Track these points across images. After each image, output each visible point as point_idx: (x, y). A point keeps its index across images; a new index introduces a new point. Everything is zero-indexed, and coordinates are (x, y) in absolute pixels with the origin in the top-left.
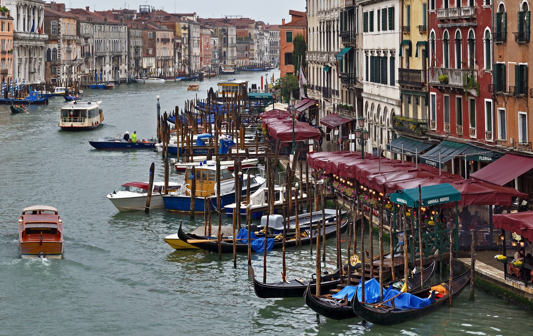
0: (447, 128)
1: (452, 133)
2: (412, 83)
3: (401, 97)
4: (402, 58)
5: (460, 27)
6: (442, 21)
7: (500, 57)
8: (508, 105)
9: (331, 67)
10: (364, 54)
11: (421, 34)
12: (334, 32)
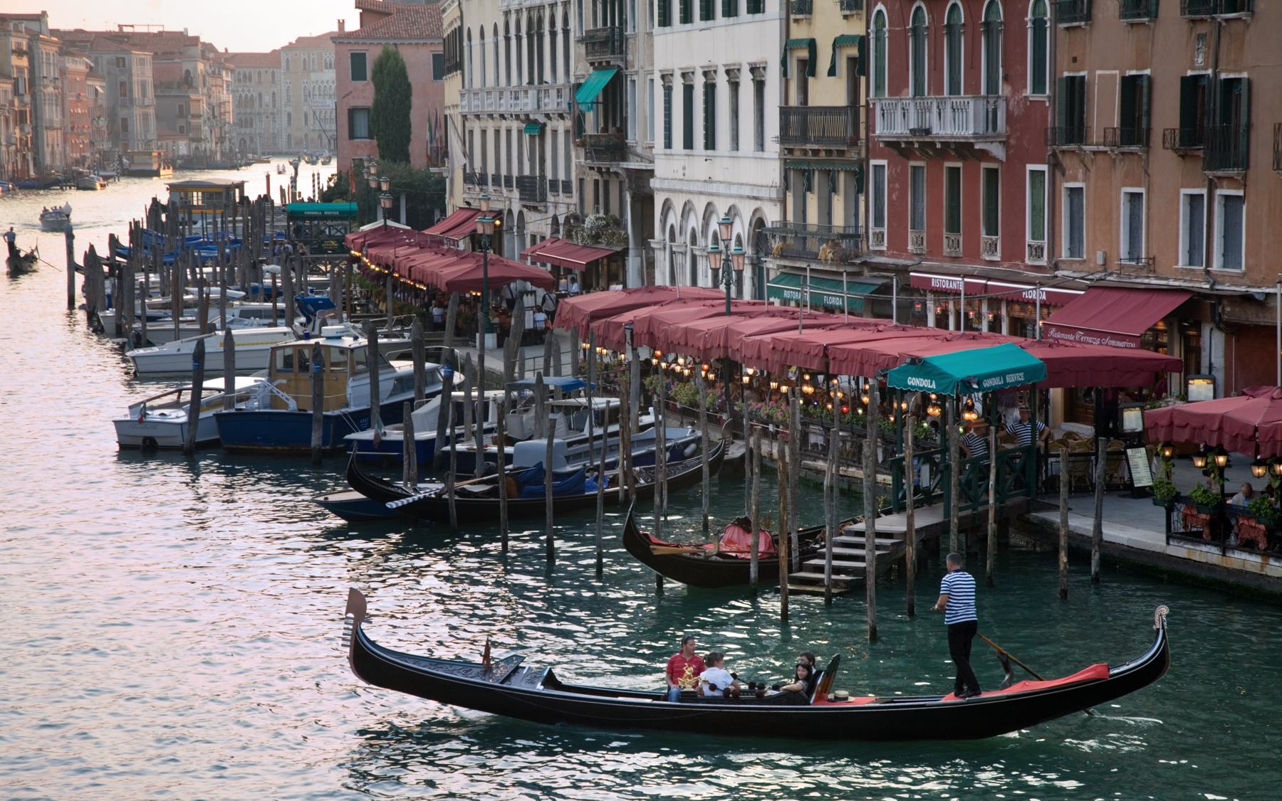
0: (919, 242)
1: (930, 252)
2: (817, 141)
3: (786, 178)
4: (787, 82)
7: (1075, 60)
8: (1092, 175)
9: (545, 125)
10: (659, 83)
11: (846, 17)
12: (553, 34)
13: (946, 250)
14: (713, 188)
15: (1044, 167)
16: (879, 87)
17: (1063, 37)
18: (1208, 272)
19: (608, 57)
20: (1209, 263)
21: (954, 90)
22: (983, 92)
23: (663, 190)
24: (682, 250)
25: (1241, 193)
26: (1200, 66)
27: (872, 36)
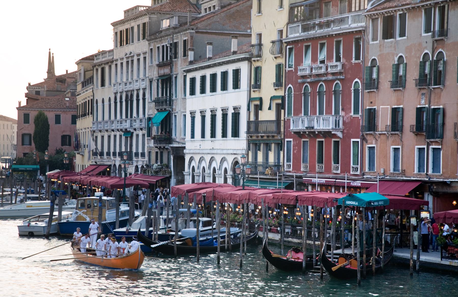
1: (310, 171)
3: (249, 146)
4: (250, 112)
5: (324, 81)
6: (303, 77)
8: (379, 142)
9: (133, 133)
11: (275, 89)
12: (138, 100)
13: (317, 170)
14: (215, 152)
15: (359, 140)
16: (289, 114)
17: (367, 95)
18: (427, 174)
19: (165, 107)
20: (427, 171)
21: (321, 113)
22: (333, 113)
23: (190, 153)
24: (198, 174)
25: (440, 147)
26: (423, 103)
27: (287, 96)
